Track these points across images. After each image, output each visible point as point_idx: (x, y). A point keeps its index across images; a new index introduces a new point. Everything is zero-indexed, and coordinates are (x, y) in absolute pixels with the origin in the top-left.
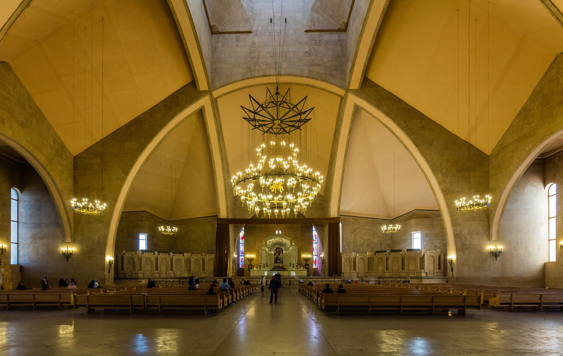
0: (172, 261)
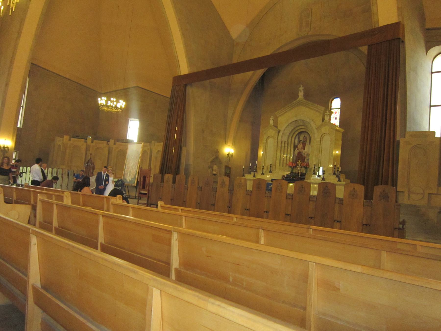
0: (110, 152)
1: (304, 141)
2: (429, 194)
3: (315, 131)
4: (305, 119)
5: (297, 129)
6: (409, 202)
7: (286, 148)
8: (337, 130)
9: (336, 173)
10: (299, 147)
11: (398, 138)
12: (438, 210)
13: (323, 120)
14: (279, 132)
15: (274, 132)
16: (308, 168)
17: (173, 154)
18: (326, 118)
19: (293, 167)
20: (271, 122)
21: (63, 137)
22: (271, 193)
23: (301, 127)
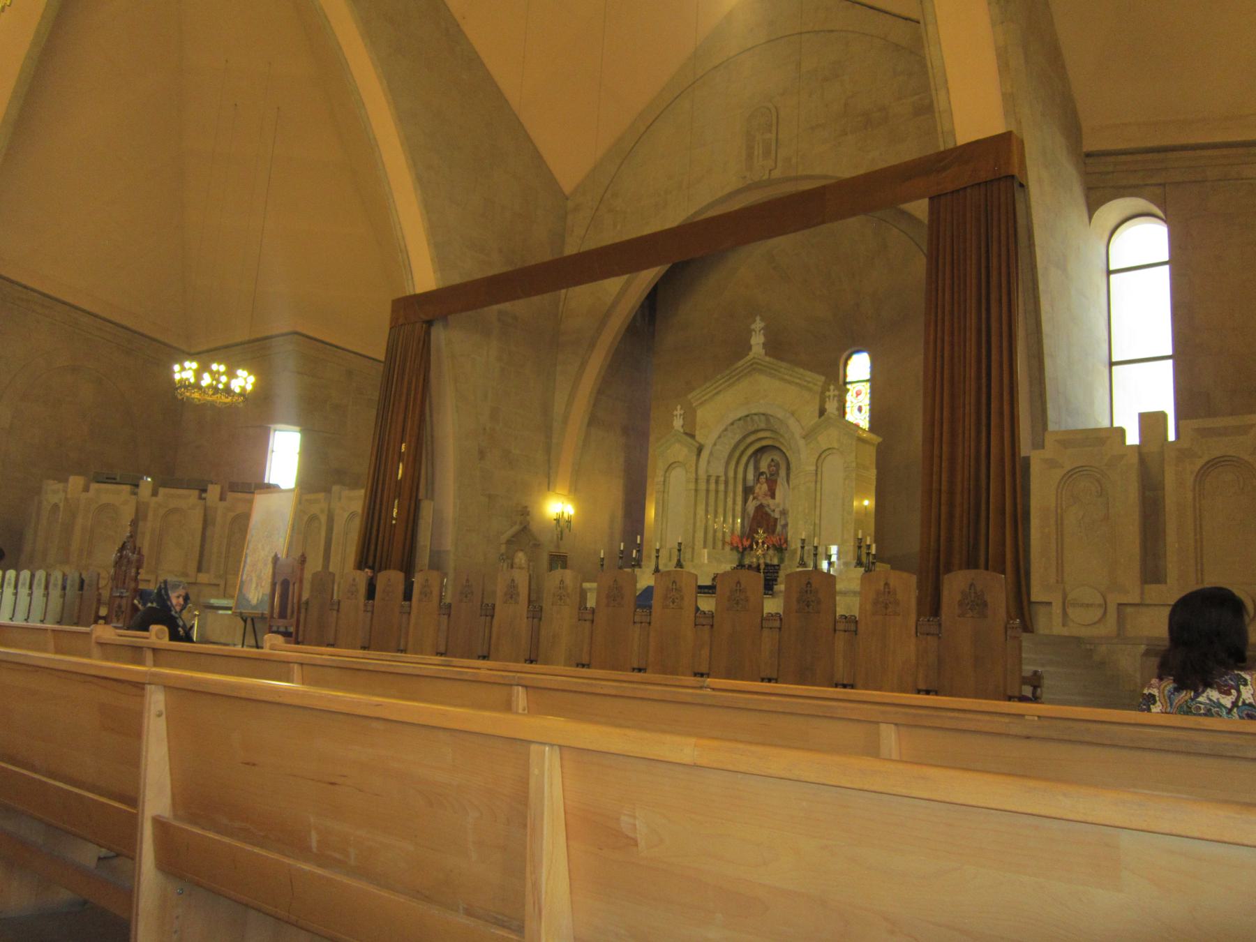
1: (771, 475)
2: (1120, 605)
3: (801, 442)
4: (769, 412)
5: (752, 438)
6: (1065, 632)
7: (721, 495)
8: (860, 440)
9: (864, 559)
10: (757, 490)
11: (1025, 449)
12: (1143, 648)
13: (822, 412)
14: (700, 450)
15: (685, 450)
16: (786, 549)
17: (394, 522)
18: (831, 407)
19: (744, 549)
20: (678, 423)
21: (66, 481)
22: (650, 612)
23: (761, 435)
